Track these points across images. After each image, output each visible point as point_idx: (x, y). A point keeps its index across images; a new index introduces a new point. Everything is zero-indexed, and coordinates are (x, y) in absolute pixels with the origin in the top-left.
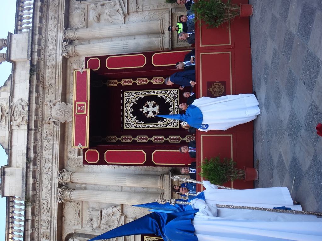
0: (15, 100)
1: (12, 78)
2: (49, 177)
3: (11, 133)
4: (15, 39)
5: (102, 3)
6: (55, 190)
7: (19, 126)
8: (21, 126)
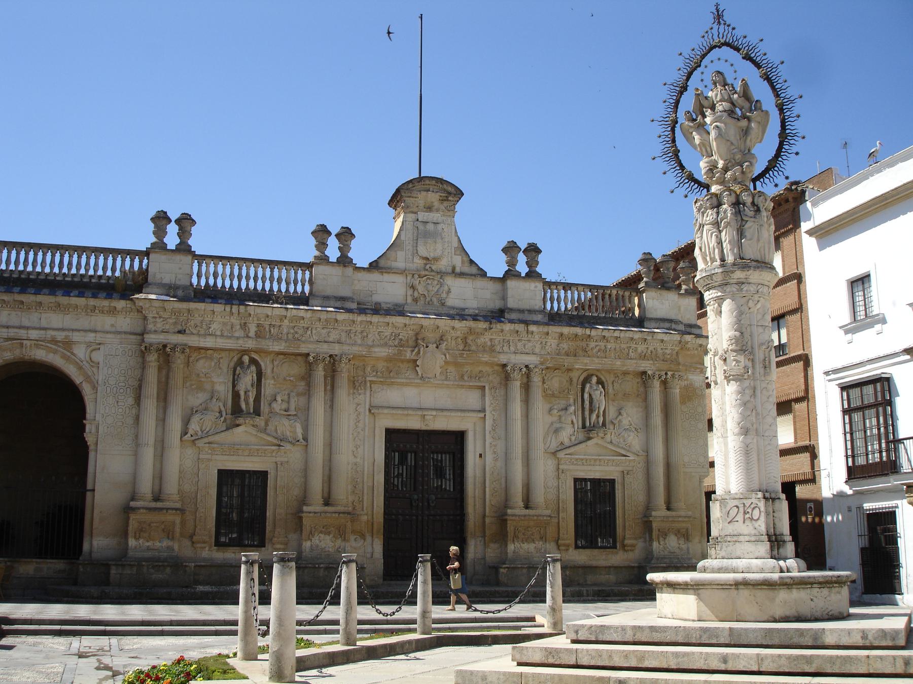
0: (449, 281)
1: (483, 274)
2: (343, 339)
3: (403, 272)
4: (536, 287)
5: (575, 421)
6: (325, 349)
7: (413, 287)
8: (412, 290)
